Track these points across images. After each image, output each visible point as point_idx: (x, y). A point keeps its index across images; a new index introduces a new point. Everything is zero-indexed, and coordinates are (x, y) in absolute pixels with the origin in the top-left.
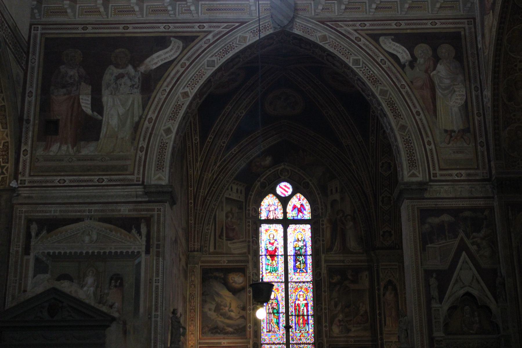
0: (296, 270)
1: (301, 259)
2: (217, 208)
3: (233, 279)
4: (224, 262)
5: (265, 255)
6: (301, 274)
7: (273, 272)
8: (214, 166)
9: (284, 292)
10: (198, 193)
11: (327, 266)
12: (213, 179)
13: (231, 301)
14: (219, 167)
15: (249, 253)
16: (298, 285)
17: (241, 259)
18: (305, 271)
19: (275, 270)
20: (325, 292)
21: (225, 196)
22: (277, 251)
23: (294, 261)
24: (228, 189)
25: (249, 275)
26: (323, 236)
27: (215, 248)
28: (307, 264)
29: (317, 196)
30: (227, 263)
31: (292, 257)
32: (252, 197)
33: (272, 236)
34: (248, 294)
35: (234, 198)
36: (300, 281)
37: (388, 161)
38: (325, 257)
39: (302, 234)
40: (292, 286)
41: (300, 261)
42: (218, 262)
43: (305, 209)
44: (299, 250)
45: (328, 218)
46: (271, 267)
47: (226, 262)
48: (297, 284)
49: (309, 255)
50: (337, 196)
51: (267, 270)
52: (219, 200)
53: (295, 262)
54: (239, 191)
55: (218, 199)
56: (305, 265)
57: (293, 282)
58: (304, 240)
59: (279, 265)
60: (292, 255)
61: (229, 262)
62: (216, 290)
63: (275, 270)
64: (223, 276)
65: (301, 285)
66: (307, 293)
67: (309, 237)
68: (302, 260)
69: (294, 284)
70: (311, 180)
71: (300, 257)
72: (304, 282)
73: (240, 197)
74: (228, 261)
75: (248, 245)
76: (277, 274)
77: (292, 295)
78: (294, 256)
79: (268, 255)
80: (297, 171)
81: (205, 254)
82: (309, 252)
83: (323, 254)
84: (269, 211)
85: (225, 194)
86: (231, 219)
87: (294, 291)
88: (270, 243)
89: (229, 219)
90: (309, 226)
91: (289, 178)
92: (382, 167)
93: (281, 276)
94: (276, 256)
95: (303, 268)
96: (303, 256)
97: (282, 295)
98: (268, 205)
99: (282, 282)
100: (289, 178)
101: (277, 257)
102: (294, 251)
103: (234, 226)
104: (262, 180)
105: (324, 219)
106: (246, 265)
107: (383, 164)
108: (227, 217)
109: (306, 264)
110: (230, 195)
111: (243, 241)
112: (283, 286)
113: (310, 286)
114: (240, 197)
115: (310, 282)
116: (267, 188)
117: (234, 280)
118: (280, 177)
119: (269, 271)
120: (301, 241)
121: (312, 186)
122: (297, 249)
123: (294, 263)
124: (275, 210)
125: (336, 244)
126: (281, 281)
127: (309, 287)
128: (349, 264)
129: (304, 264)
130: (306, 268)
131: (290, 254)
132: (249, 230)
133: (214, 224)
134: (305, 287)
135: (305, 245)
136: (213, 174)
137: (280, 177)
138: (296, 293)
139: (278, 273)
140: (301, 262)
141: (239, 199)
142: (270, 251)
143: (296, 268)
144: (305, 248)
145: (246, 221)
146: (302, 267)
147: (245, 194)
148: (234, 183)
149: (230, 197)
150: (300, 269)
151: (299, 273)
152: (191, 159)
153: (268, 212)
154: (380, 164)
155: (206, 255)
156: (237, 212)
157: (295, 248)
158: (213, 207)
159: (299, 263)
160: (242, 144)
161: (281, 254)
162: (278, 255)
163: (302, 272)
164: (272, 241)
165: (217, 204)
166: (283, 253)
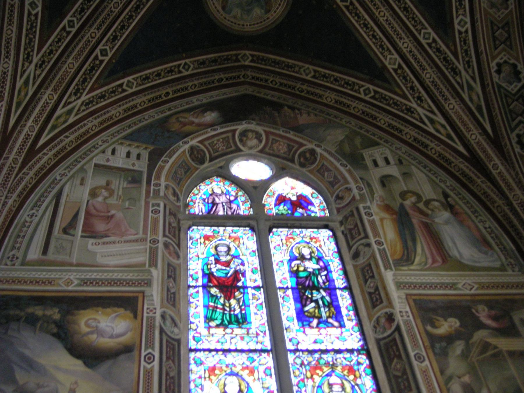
0: (306, 321)
1: (319, 296)
2: (68, 180)
3: (94, 324)
4: (69, 282)
5: (204, 286)
6: (323, 331)
7: (230, 326)
8: (73, 98)
9: (274, 376)
10: (19, 128)
11: (407, 295)
12: (65, 122)
13: (76, 383)
14: (87, 104)
15: (153, 263)
16: (321, 358)
17: (130, 276)
18: (336, 324)
19: (237, 321)
20: (419, 357)
21: (95, 161)
22: (243, 279)
23: (295, 300)
24: (103, 152)
25: (151, 314)
26: (376, 234)
27: (45, 251)
28: (340, 307)
29: (342, 169)
30: (79, 285)
31: (289, 292)
32: (168, 166)
33: (223, 249)
34: (143, 363)
35: (120, 165)
36: (323, 348)
37: (510, 59)
38: (394, 275)
39: (310, 245)
40: (299, 361)
41: (316, 302)
42: (50, 282)
43: (312, 204)
44: (306, 277)
45: (379, 203)
46: (224, 314)
47: (76, 282)
48: (317, 355)
49: (340, 289)
50: (393, 170)
51: (211, 319)
52: (79, 166)
53: (301, 302)
54: (134, 155)
55: (75, 165)
56: (332, 309)
57: (303, 351)
58: (319, 259)
59: (252, 310)
60: (287, 288)
61: (84, 282)
62: (27, 352)
63: (237, 321)
64: (57, 316)
65: (328, 357)
66: (356, 378)
67: (331, 252)
68: (322, 298)
69: (307, 358)
70: (318, 146)
71: (314, 292)
72: (339, 351)
73: (134, 165)
74: (82, 280)
75: (151, 248)
76: (244, 331)
77: (301, 384)
78: (297, 291)
79: (215, 286)
80: (281, 132)
81: (9, 263)
82: (339, 282)
83: (386, 269)
84: (214, 204)
85: (94, 159)
86: (106, 198)
87: (309, 375)
88: (217, 261)
89: (100, 199)
90: (326, 233)
91: (262, 151)
92: (499, 72)
93: (258, 334)
94: (238, 288)
95: (329, 317)
96: (322, 291)
97: (266, 386)
98: (211, 195)
99: (262, 351)
100: (262, 151)
101: (242, 290)
102: (294, 280)
103: (113, 212)
104: (194, 142)
105: (368, 204)
106: (143, 292)
107: (499, 65)
108: (93, 194)
109: (338, 309)
110: (108, 160)
111: (136, 241)
112: (268, 360)
113: (361, 361)
114: (134, 165)
115: (357, 350)
116: (206, 164)
117: (97, 327)
118: (239, 150)
119: (218, 322)
120: (310, 259)
121: (325, 154)
122: (302, 274)
123: (299, 305)
124: (231, 202)
125: (419, 250)
126: (259, 347)
127: (359, 364)
128: (473, 292)
129: (329, 307)
130: (338, 315)
131: (281, 286)
132: (155, 222)
133: (51, 209)
134: (345, 362)
135: (326, 268)
136: (69, 112)
137: (240, 150)
138: (317, 379)
139: (248, 330)
140: (321, 303)
141: (131, 167)
142: (218, 279)
143: (307, 316)
144: (325, 273)
145: (147, 203)
146: (324, 315)
147: (149, 160)
148: (122, 144)
149: (108, 164)
150: (320, 318)
151: (317, 327)
152: (14, 35)
153: (210, 205)
154: (493, 64)
155: (14, 265)
156: (123, 188)
157: (295, 273)
158: (58, 178)
159: (313, 305)
160: (147, 78)
161: (253, 285)
162: (245, 287)
163: (328, 327)
164: (223, 259)
165: (69, 175)
166: (259, 283)
